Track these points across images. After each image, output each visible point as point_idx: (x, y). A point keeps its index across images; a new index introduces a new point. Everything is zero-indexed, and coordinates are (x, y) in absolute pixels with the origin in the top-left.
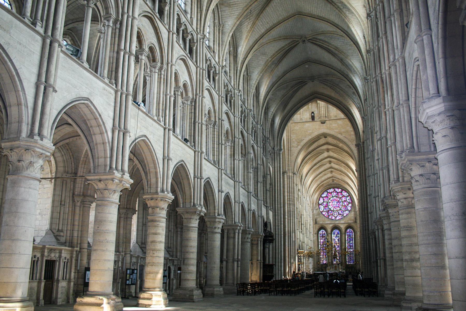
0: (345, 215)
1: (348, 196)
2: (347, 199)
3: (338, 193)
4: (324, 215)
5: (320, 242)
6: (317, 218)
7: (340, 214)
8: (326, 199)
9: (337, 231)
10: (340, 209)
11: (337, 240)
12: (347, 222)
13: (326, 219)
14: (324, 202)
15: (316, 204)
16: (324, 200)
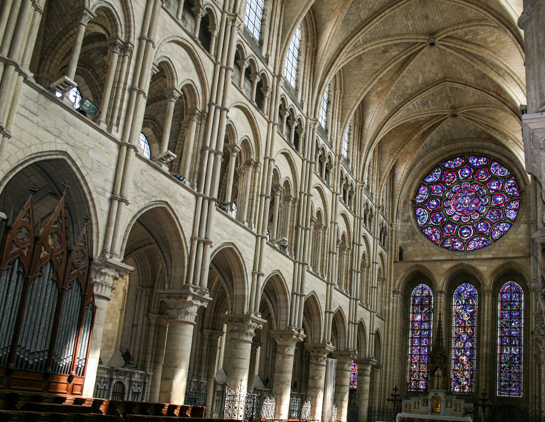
0: (497, 234)
1: (506, 179)
2: (506, 185)
3: (476, 170)
4: (428, 237)
5: (413, 321)
6: (406, 246)
7: (482, 234)
8: (438, 190)
9: (470, 288)
10: (482, 220)
11: (466, 318)
12: (501, 256)
13: (433, 248)
14: (431, 198)
15: (405, 203)
16: (431, 191)
